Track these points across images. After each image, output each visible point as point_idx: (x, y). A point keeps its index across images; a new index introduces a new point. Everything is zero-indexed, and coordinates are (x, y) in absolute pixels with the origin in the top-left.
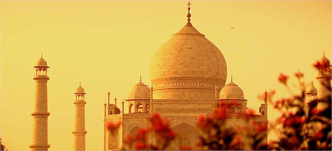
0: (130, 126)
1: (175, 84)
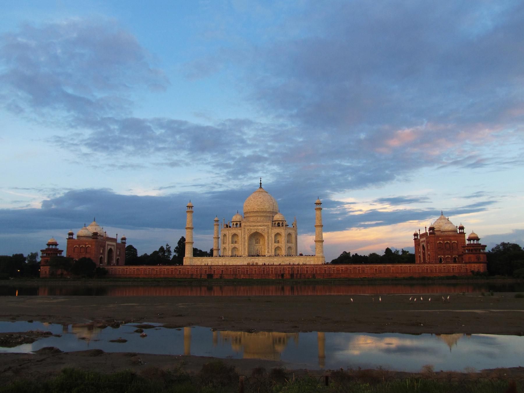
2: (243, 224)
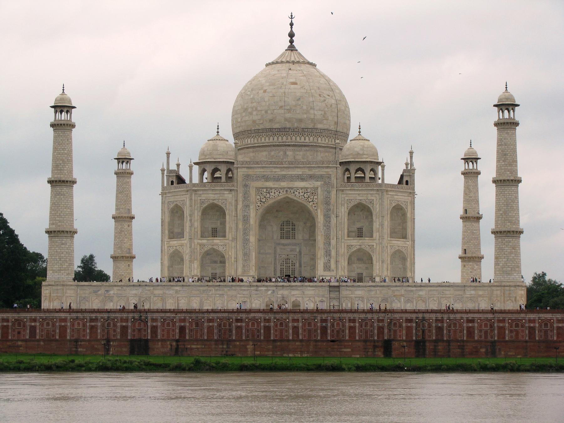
0: (202, 202)
1: (271, 138)
2: (240, 173)
